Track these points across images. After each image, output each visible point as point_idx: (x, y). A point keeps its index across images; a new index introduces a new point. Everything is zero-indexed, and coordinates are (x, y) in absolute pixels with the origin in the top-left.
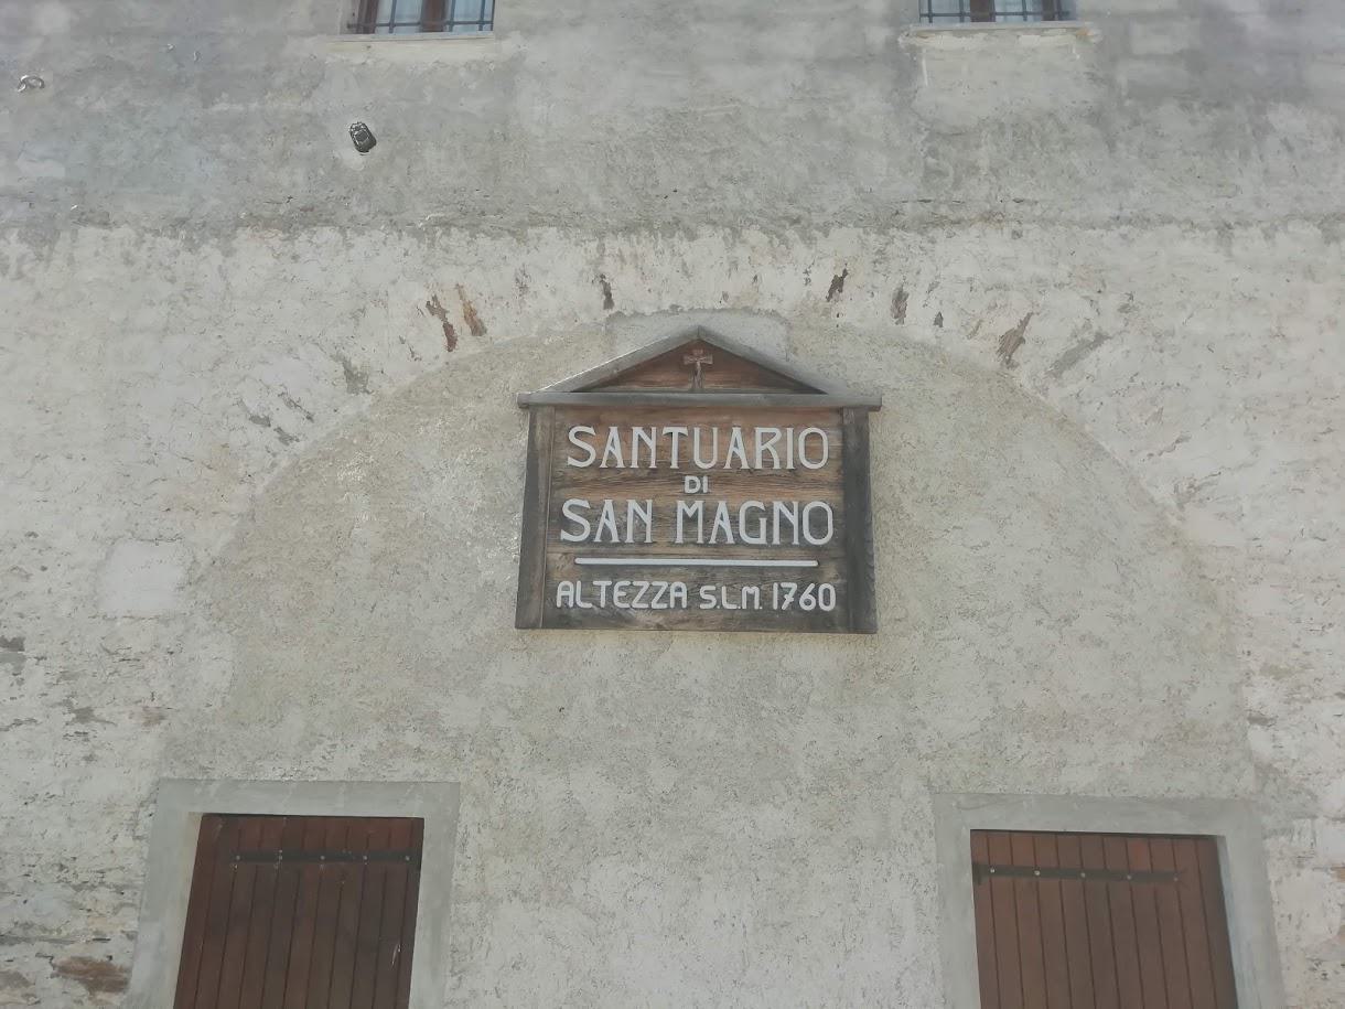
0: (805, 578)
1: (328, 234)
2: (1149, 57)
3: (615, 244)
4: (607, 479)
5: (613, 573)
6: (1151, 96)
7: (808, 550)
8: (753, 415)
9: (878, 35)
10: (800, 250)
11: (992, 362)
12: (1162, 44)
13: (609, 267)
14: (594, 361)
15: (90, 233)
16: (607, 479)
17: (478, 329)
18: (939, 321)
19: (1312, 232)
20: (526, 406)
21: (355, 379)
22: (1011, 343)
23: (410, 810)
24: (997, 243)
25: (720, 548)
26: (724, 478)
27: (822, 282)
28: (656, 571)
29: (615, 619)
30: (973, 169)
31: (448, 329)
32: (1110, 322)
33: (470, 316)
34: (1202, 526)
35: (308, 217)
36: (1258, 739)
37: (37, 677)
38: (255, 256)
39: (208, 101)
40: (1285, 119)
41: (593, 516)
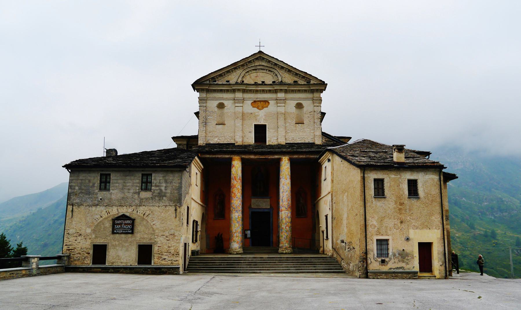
0: (129, 230)
1: (99, 206)
2: (156, 193)
3: (118, 207)
5: (118, 230)
6: (155, 196)
7: (130, 229)
8: (127, 220)
9: (137, 191)
10: (131, 208)
12: (157, 192)
13: (118, 209)
14: (117, 216)
15: (82, 206)
17: (109, 213)
18: (140, 213)
19: (164, 207)
21: (101, 217)
22: (144, 214)
24: (144, 207)
25: (125, 228)
26: (125, 224)
27: (132, 210)
28: (121, 230)
30: (143, 202)
31: (107, 213)
33: (109, 212)
34: (154, 227)
35: (97, 205)
36: (155, 239)
37: (82, 237)
38: (94, 208)
39: (89, 195)
40: (164, 198)
41: (117, 226)
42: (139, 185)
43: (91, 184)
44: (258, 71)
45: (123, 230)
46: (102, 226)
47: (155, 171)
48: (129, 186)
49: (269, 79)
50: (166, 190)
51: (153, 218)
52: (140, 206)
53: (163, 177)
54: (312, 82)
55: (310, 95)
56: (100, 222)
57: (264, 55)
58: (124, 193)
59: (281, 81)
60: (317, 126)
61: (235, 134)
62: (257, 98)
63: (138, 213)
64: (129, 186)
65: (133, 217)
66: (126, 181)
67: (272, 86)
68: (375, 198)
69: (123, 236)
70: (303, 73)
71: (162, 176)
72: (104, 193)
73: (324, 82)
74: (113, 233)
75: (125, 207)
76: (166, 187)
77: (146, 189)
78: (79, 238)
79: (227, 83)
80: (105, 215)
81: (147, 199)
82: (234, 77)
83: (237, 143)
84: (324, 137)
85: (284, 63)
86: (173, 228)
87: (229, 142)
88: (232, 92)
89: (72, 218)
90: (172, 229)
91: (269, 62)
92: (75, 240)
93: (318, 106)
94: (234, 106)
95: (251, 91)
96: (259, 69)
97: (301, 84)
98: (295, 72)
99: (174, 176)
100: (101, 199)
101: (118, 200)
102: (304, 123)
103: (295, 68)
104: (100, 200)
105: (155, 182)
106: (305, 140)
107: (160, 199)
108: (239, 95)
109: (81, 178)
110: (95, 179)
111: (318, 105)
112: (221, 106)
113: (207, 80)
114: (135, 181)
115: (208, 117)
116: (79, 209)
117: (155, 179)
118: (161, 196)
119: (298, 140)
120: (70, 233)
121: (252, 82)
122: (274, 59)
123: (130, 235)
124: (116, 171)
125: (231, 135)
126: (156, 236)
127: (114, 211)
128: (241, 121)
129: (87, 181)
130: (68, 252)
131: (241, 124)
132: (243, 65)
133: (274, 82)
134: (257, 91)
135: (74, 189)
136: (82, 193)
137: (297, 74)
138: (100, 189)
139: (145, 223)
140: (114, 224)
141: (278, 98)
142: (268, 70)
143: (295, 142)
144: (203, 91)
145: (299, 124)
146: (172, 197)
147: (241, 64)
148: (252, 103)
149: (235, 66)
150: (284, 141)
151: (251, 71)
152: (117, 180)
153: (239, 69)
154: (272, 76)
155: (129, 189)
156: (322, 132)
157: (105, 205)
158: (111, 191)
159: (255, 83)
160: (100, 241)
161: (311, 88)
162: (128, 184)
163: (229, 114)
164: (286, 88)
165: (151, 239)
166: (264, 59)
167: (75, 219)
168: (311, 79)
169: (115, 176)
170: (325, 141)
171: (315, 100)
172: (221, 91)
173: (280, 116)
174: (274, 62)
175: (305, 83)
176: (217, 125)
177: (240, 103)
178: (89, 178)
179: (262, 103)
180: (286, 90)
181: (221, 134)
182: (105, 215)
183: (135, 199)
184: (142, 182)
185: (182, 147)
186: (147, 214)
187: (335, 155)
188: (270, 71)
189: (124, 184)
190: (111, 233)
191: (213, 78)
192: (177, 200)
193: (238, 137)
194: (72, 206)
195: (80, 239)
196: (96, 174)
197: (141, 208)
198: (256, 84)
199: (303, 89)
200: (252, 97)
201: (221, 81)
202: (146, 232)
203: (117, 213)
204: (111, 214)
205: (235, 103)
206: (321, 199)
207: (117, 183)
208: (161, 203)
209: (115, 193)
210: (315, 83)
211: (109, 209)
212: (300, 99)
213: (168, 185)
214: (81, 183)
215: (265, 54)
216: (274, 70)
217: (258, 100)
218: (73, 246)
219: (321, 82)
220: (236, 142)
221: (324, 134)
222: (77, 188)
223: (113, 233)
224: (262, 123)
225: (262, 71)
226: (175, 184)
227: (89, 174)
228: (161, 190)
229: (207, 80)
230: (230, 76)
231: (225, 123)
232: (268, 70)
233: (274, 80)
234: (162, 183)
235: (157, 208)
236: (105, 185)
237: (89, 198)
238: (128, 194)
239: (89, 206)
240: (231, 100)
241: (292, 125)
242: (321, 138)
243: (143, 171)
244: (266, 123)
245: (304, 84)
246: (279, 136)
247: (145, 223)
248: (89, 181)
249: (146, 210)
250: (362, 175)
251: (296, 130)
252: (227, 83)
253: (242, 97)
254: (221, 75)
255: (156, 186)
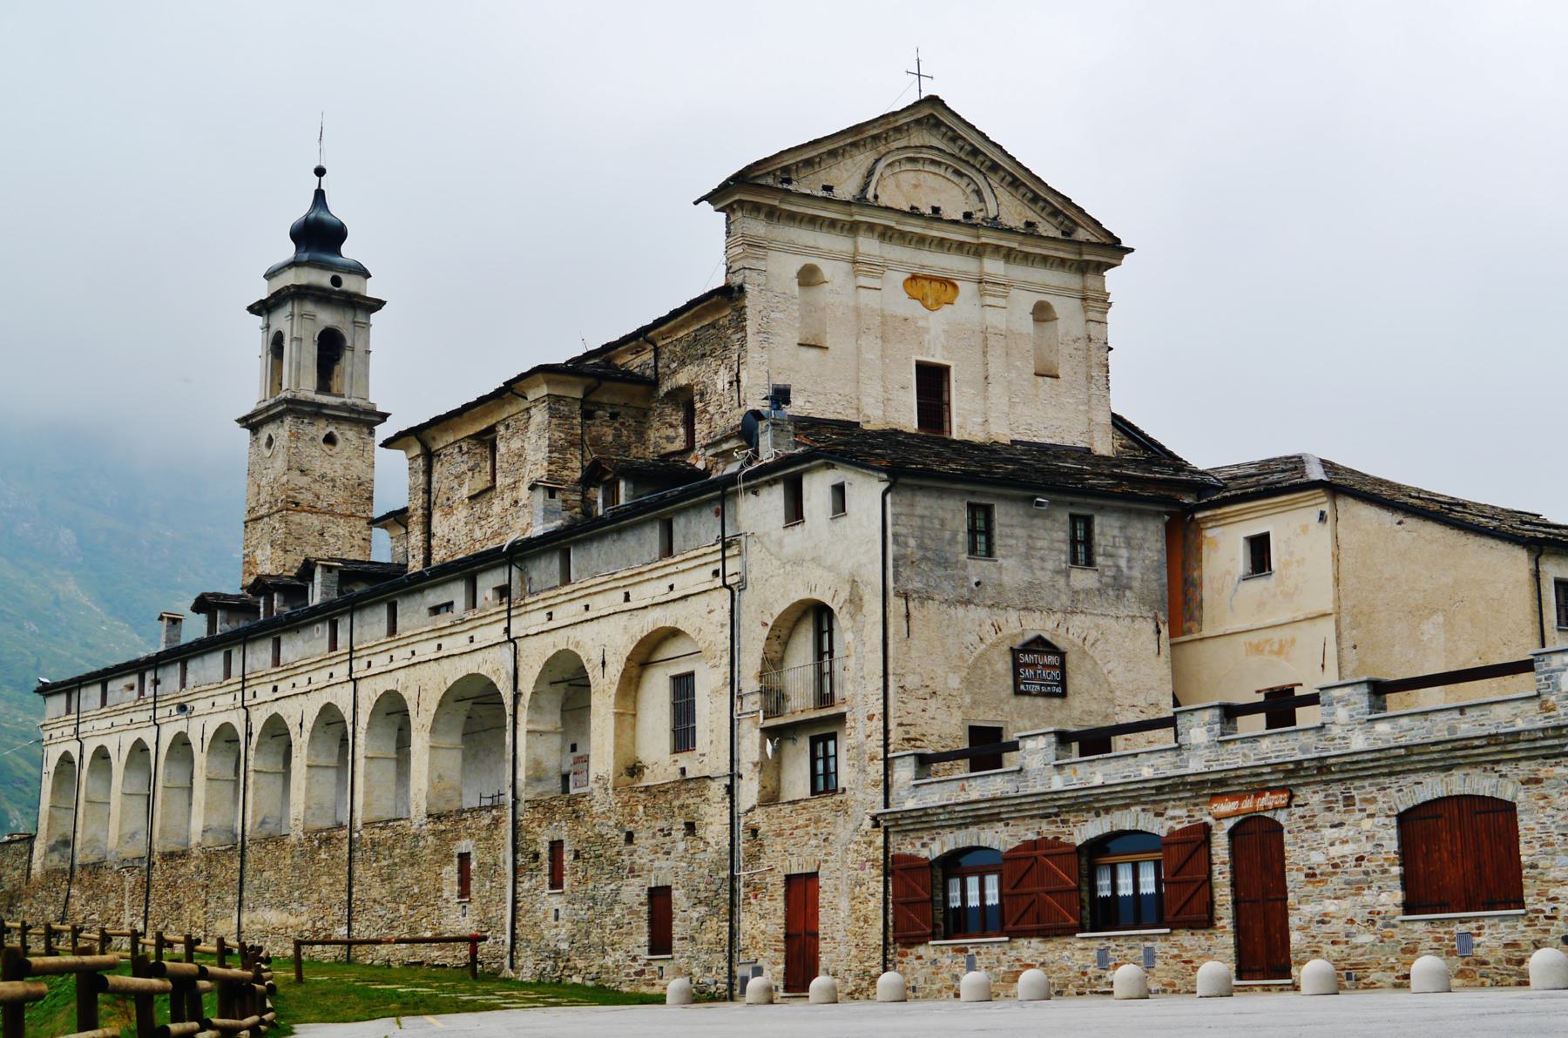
0: (1057, 686)
3: (1022, 612)
4: (1026, 665)
6: (1107, 585)
8: (1048, 653)
9: (1064, 566)
11: (1081, 644)
15: (930, 601)
16: (1026, 665)
19: (1130, 620)
20: (1012, 649)
22: (1085, 639)
23: (1000, 725)
25: (1044, 680)
26: (1044, 666)
29: (1028, 693)
32: (1100, 637)
34: (1111, 679)
35: (968, 602)
37: (940, 698)
38: (961, 611)
39: (946, 568)
40: (1128, 593)
42: (1066, 547)
43: (947, 535)
44: (920, 166)
45: (1041, 685)
46: (987, 667)
47: (1101, 509)
48: (1041, 549)
49: (953, 199)
50: (1130, 568)
51: (1108, 653)
52: (1072, 612)
53: (1121, 528)
54: (1081, 235)
55: (1072, 280)
56: (982, 655)
57: (945, 112)
58: (1031, 568)
59: (995, 218)
60: (1098, 393)
61: (858, 387)
62: (923, 267)
63: (1070, 636)
64: (1041, 549)
65: (1061, 644)
66: (1033, 531)
67: (973, 231)
68: (1559, 630)
69: (1040, 701)
70: (1060, 200)
71: (1118, 524)
72: (983, 565)
73: (1119, 241)
74: (1018, 692)
75: (1038, 613)
76: (1129, 560)
77: (1090, 562)
78: (932, 704)
79: (825, 194)
80: (991, 638)
81: (1087, 592)
82: (849, 177)
83: (868, 422)
84: (1119, 433)
85: (1005, 153)
86: (1155, 686)
87: (840, 417)
88: (845, 233)
89: (910, 641)
90: (1152, 688)
91: (955, 138)
92: (923, 711)
93: (1100, 322)
94: (851, 287)
95: (904, 238)
96: (925, 160)
97: (1045, 234)
98: (1032, 191)
99: (1145, 529)
100: (978, 584)
101: (1019, 591)
102: (1057, 377)
103: (1038, 179)
104: (974, 586)
105: (1103, 543)
106: (1063, 435)
107: (1117, 597)
108: (869, 246)
109: (919, 511)
110: (951, 514)
111: (1098, 316)
112: (808, 277)
113: (768, 173)
114: (1055, 535)
115: (773, 315)
116: (925, 612)
117: (1102, 534)
118: (1119, 585)
119: (1043, 432)
120: (907, 686)
121: (904, 203)
122: (974, 135)
123: (1057, 702)
124: (1013, 499)
125: (847, 390)
126: (1118, 709)
127: (1012, 625)
128: (879, 341)
129: (937, 524)
130: (906, 745)
131: (879, 354)
132: (875, 138)
133: (968, 215)
134: (922, 241)
135: (906, 545)
136: (925, 558)
137: (1036, 199)
138: (973, 551)
139: (1088, 665)
140: (1017, 666)
141: (989, 274)
142: (950, 170)
143: (1036, 440)
144: (755, 214)
145: (1046, 379)
146: (1146, 592)
147: (875, 132)
148: (907, 280)
149: (856, 137)
150: (1007, 432)
151: (899, 161)
152: (1012, 526)
153: (862, 149)
154: (964, 192)
155: (1042, 559)
156: (1114, 415)
157: (989, 602)
158: (1000, 560)
159: (912, 208)
160: (985, 718)
161: (1086, 257)
162: (1040, 544)
163: (839, 314)
164: (1015, 245)
165: (1107, 716)
166: (939, 124)
167: (915, 642)
168: (1077, 224)
169: (1006, 514)
170: (1121, 445)
171: (1093, 300)
172: (813, 221)
173: (992, 340)
174: (971, 144)
175: (1058, 234)
176: (802, 348)
177: (873, 277)
178: (940, 513)
179: (936, 285)
180: (1011, 249)
181: (816, 382)
182: (991, 638)
183: (1059, 591)
184: (1074, 542)
185: (566, 409)
186: (1090, 639)
187: (1350, 501)
188: (957, 173)
189: (1030, 541)
190: (1011, 690)
191: (786, 169)
192: (1157, 601)
193: (872, 400)
194: (904, 602)
195: (934, 707)
196: (959, 503)
197: (1078, 623)
198: (914, 213)
199: (1061, 255)
200: (905, 259)
201: (807, 184)
202: (1096, 695)
203: (1019, 630)
204: (1006, 632)
205: (856, 273)
206: (1201, 639)
207: (1011, 536)
208: (1121, 608)
209: (1008, 569)
210: (1093, 239)
211: (1000, 617)
212: (1045, 288)
213: (1135, 554)
214: (922, 528)
215: (949, 109)
216: (974, 171)
217: (926, 272)
218: (919, 730)
219: (1108, 241)
220: (866, 419)
221: (1117, 422)
222: (912, 542)
223: (1018, 692)
224: (938, 359)
225: (929, 168)
226: (1150, 554)
227: (940, 502)
228: (1118, 567)
229: (768, 173)
230: (834, 172)
231: (827, 345)
232: (950, 170)
233: (968, 209)
234: (1120, 547)
235: (1113, 621)
236: (981, 538)
237: (947, 577)
238: (1043, 573)
239: (948, 603)
240: (843, 260)
241: (1025, 376)
242: (1111, 436)
243: (1072, 504)
244: (951, 359)
245: (1054, 239)
246: (993, 414)
247: (1090, 666)
248: (943, 522)
249: (1088, 629)
250: (1533, 566)
251: (1037, 396)
252: (821, 193)
253: (877, 253)
254: (809, 163)
255: (1107, 555)
